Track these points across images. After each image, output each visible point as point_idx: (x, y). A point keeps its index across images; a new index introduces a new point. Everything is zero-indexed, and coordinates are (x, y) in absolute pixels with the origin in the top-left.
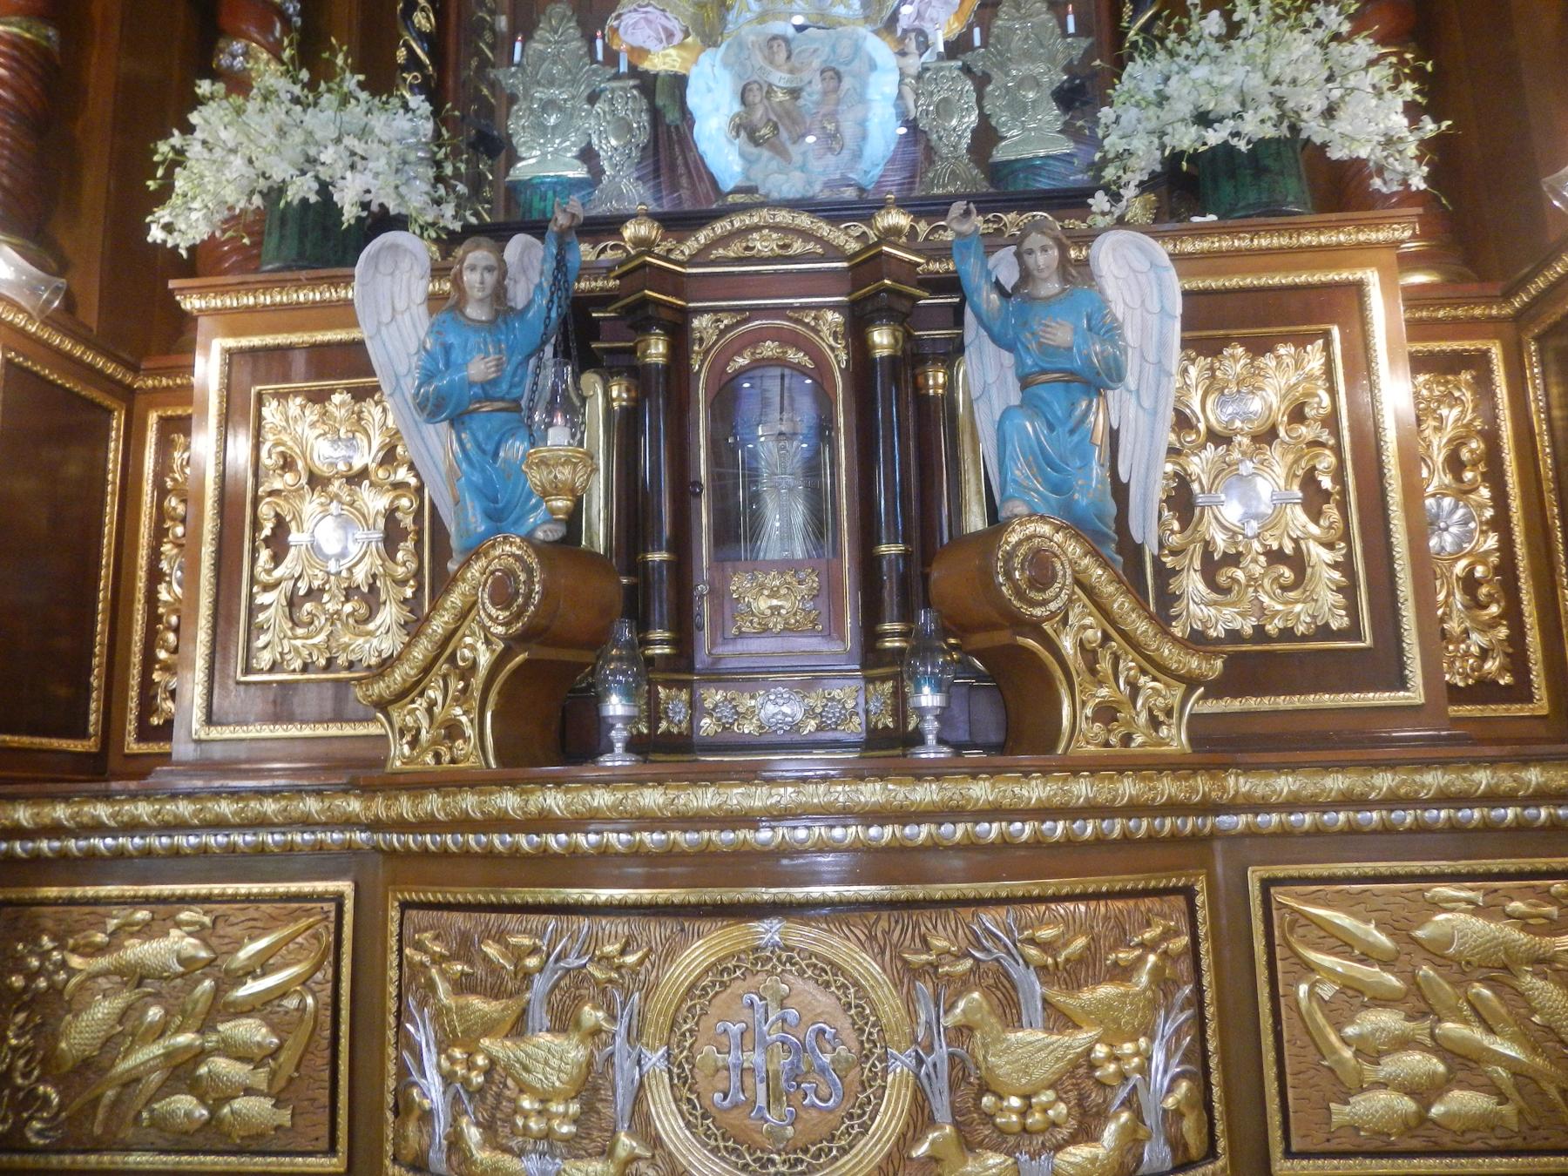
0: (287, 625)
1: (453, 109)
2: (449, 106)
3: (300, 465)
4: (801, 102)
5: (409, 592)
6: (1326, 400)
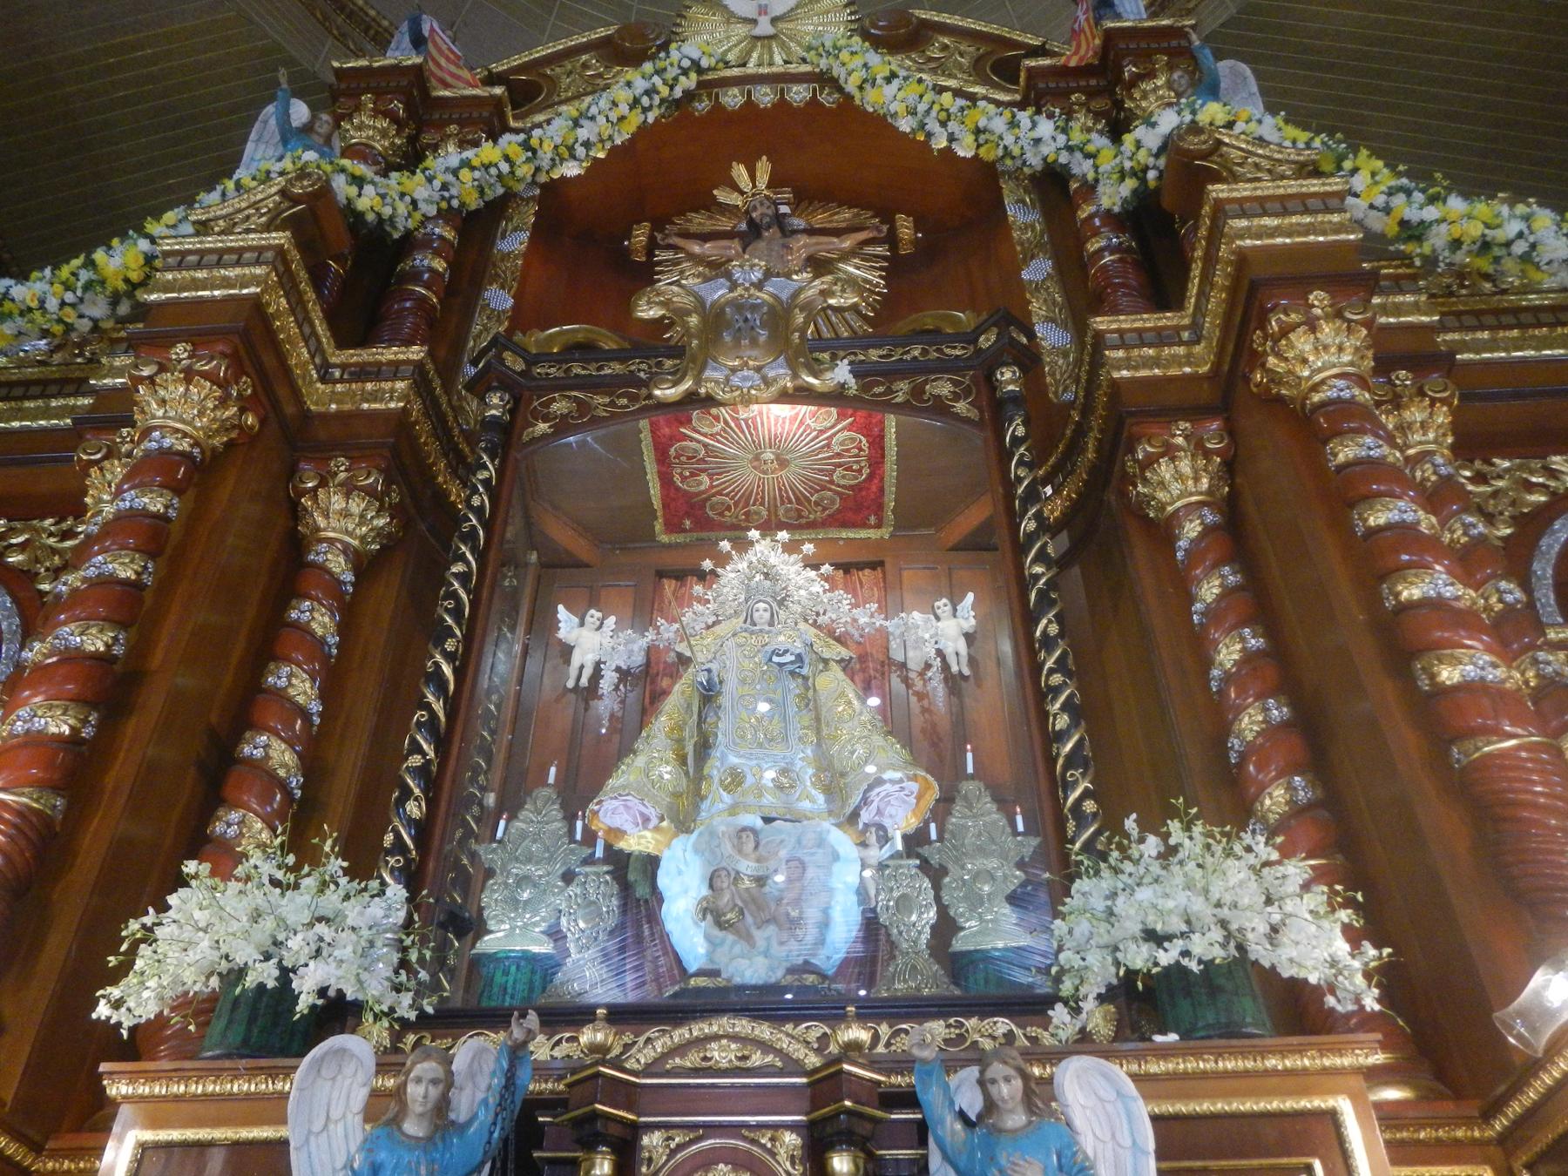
1: (428, 896)
2: (425, 892)
4: (767, 889)
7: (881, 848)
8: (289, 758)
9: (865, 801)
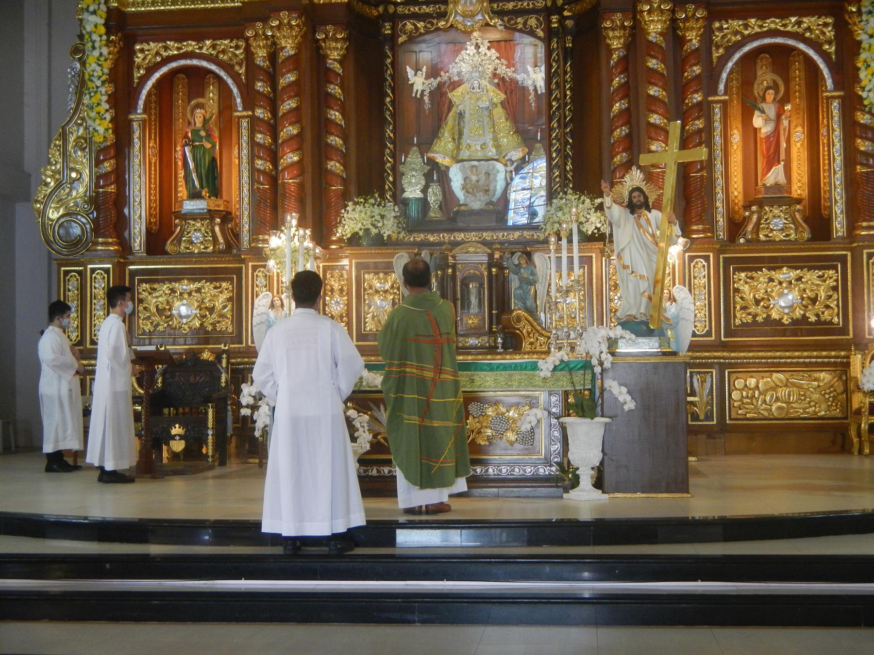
8: (341, 142)
9: (507, 154)
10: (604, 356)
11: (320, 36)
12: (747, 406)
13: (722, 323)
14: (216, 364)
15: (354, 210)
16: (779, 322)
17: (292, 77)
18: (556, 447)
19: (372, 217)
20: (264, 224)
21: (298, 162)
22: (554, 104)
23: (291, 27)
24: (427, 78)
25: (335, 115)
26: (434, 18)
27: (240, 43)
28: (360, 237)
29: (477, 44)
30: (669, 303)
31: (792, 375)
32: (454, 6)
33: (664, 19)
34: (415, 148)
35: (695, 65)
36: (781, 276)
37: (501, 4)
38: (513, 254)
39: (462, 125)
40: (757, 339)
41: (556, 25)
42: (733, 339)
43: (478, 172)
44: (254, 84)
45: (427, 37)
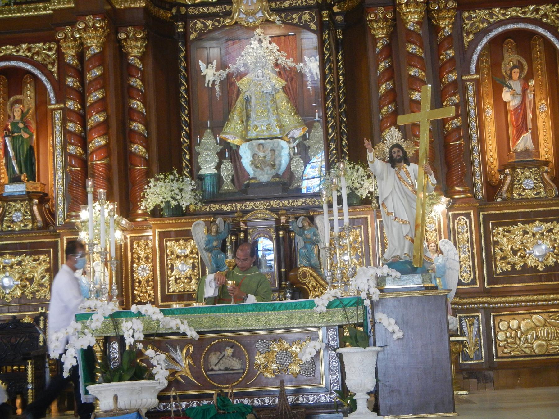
0: (175, 284)
3: (175, 254)
4: (266, 159)
5: (198, 277)
6: (360, 239)
7: (294, 143)
8: (143, 128)
9: (289, 133)
10: (372, 291)
11: (122, 36)
12: (511, 345)
13: (485, 272)
14: (34, 326)
15: (155, 186)
16: (535, 269)
17: (98, 71)
18: (336, 376)
19: (173, 191)
20: (77, 202)
21: (105, 146)
22: (328, 86)
23: (96, 29)
24: (217, 70)
25: (137, 104)
26: (220, 17)
27: (52, 46)
28: (162, 209)
29: (260, 39)
30: (436, 255)
31: (549, 316)
32: (238, 6)
33: (419, 10)
34: (208, 131)
35: (449, 49)
36: (534, 229)
37: (278, 3)
38: (297, 218)
39: (249, 109)
40: (517, 285)
41: (327, 19)
42: (495, 286)
43: (265, 149)
44: (65, 80)
45: (216, 34)
